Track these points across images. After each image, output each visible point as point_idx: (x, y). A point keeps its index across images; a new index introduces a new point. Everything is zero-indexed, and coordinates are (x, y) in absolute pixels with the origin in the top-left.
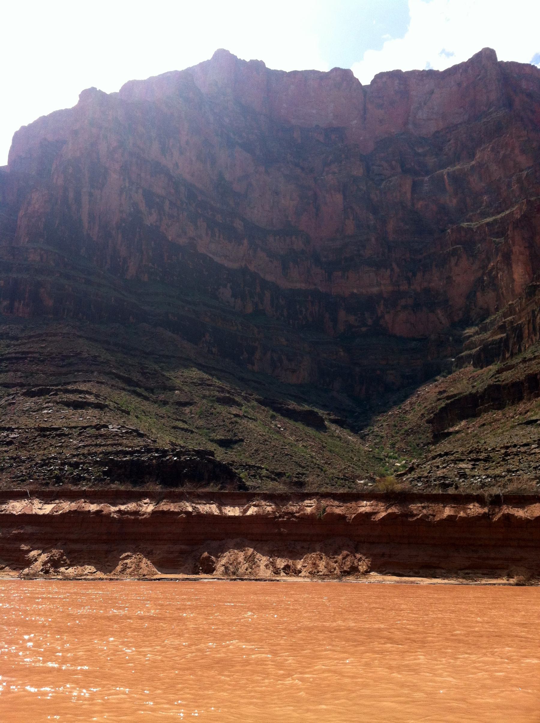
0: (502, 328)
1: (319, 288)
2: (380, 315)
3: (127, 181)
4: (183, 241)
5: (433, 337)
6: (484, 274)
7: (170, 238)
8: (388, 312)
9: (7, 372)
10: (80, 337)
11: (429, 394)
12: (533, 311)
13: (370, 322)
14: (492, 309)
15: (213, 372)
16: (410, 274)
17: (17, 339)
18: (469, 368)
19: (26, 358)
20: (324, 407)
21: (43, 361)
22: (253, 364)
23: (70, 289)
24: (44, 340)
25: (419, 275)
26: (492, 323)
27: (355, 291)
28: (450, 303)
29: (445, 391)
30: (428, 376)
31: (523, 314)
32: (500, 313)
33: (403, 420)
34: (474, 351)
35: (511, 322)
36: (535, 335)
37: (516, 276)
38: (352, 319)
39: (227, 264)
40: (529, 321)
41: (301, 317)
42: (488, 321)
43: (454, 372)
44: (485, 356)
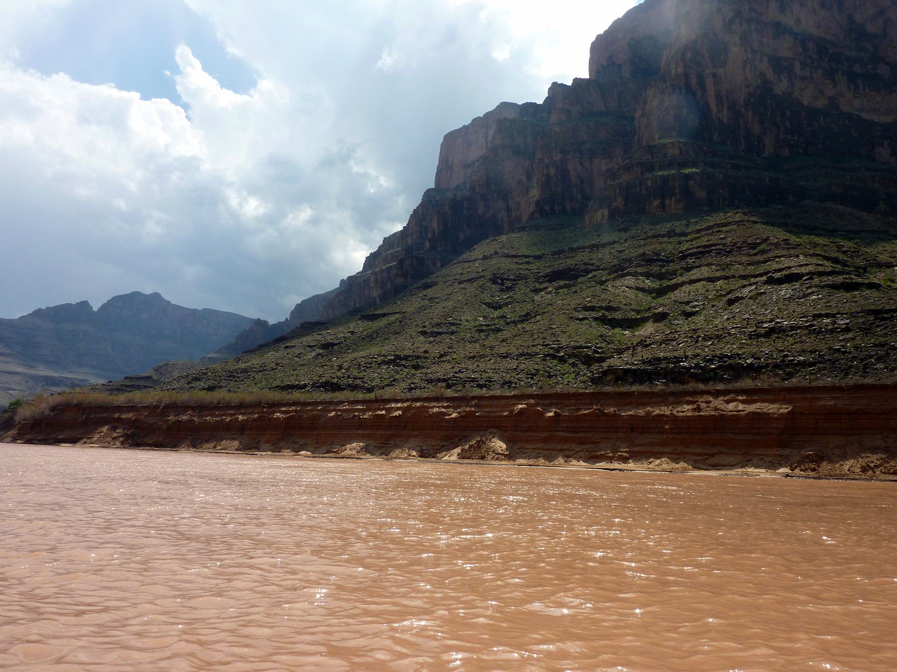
3: (749, 50)
4: (820, 103)
7: (806, 103)
9: (699, 266)
10: (755, 222)
17: (686, 235)
19: (711, 251)
21: (730, 252)
23: (721, 176)
24: (718, 231)
39: (876, 118)
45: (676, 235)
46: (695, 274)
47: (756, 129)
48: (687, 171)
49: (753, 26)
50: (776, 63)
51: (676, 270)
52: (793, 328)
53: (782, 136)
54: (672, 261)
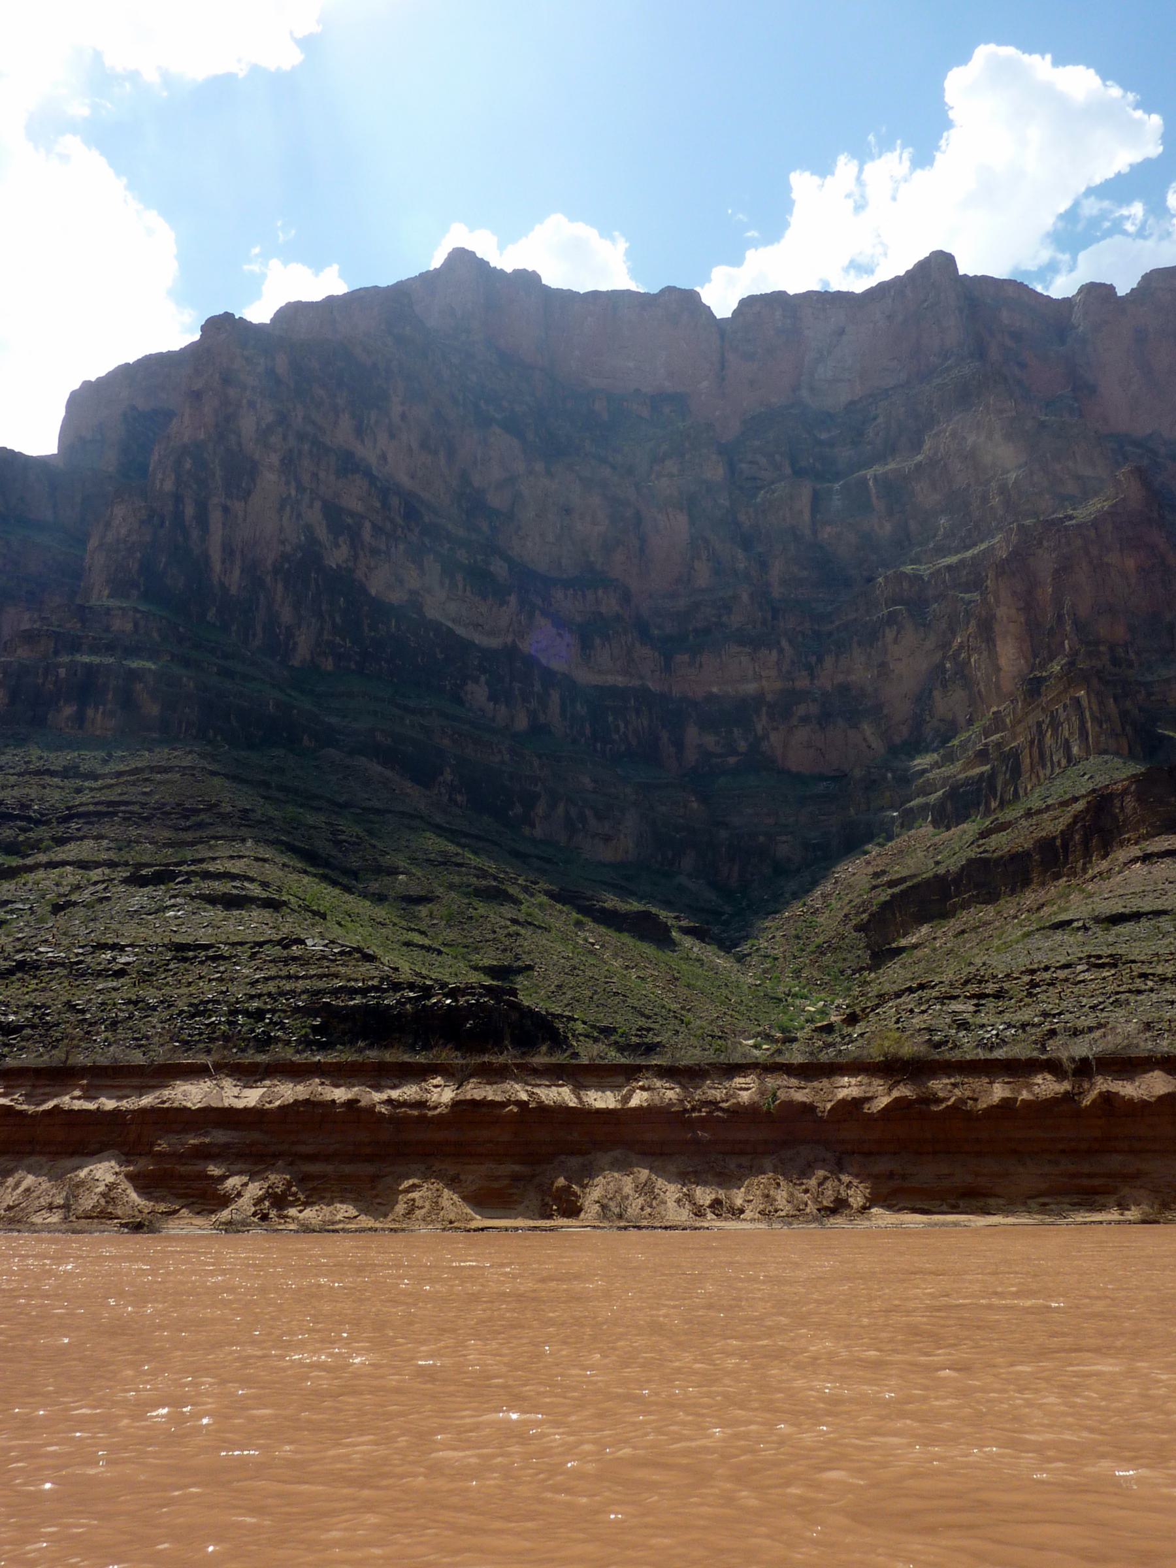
0: (982, 755)
1: (650, 684)
2: (760, 732)
5: (858, 773)
6: (944, 657)
7: (373, 592)
8: (776, 729)
11: (855, 879)
12: (1039, 724)
13: (742, 746)
14: (962, 720)
15: (463, 840)
16: (813, 659)
18: (926, 829)
20: (668, 904)
22: (533, 826)
23: (191, 684)
25: (829, 662)
26: (963, 746)
27: (715, 690)
28: (885, 711)
29: (884, 872)
30: (852, 842)
31: (1019, 729)
32: (977, 727)
33: (811, 926)
34: (932, 798)
35: (998, 745)
36: (1044, 767)
37: (1003, 662)
38: (710, 740)
39: (478, 639)
40: (1032, 742)
41: (616, 737)
42: (956, 742)
43: (898, 836)
44: (958, 805)
45: (78, 775)
46: (71, 851)
47: (286, 616)
48: (135, 664)
49: (306, 447)
50: (333, 513)
51: (41, 840)
52: (52, 964)
53: (326, 637)
54: (47, 823)
